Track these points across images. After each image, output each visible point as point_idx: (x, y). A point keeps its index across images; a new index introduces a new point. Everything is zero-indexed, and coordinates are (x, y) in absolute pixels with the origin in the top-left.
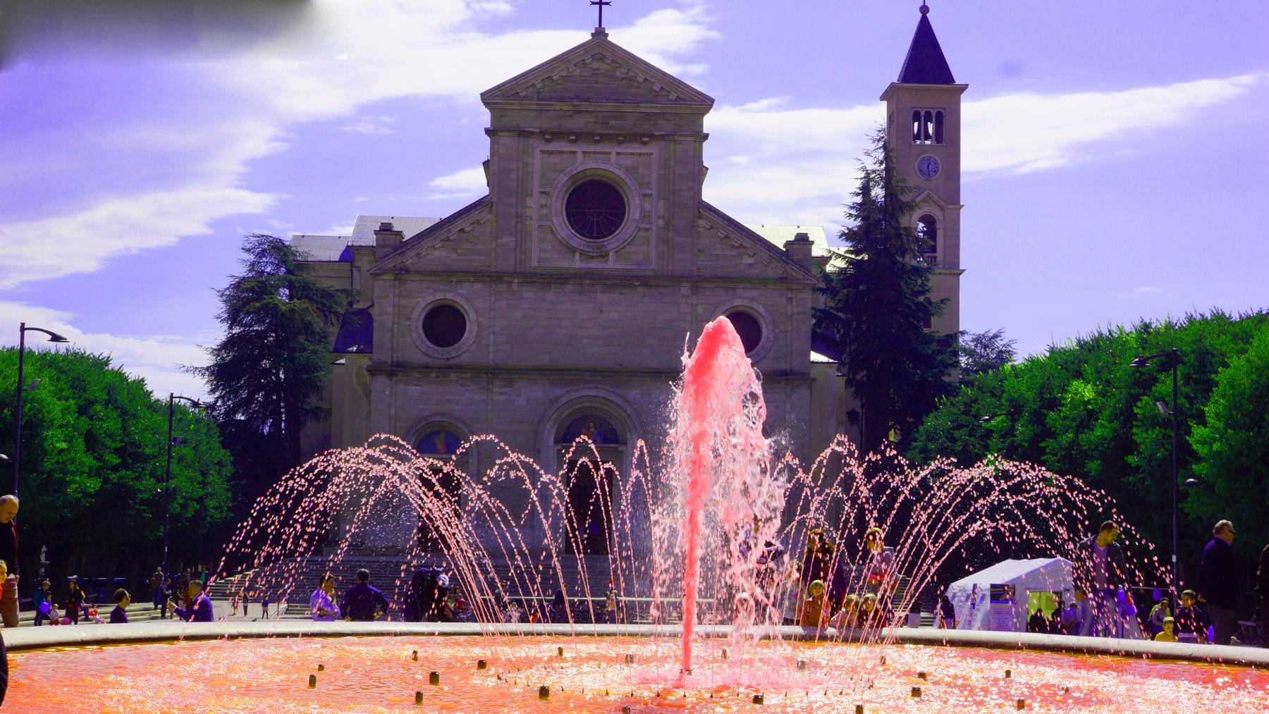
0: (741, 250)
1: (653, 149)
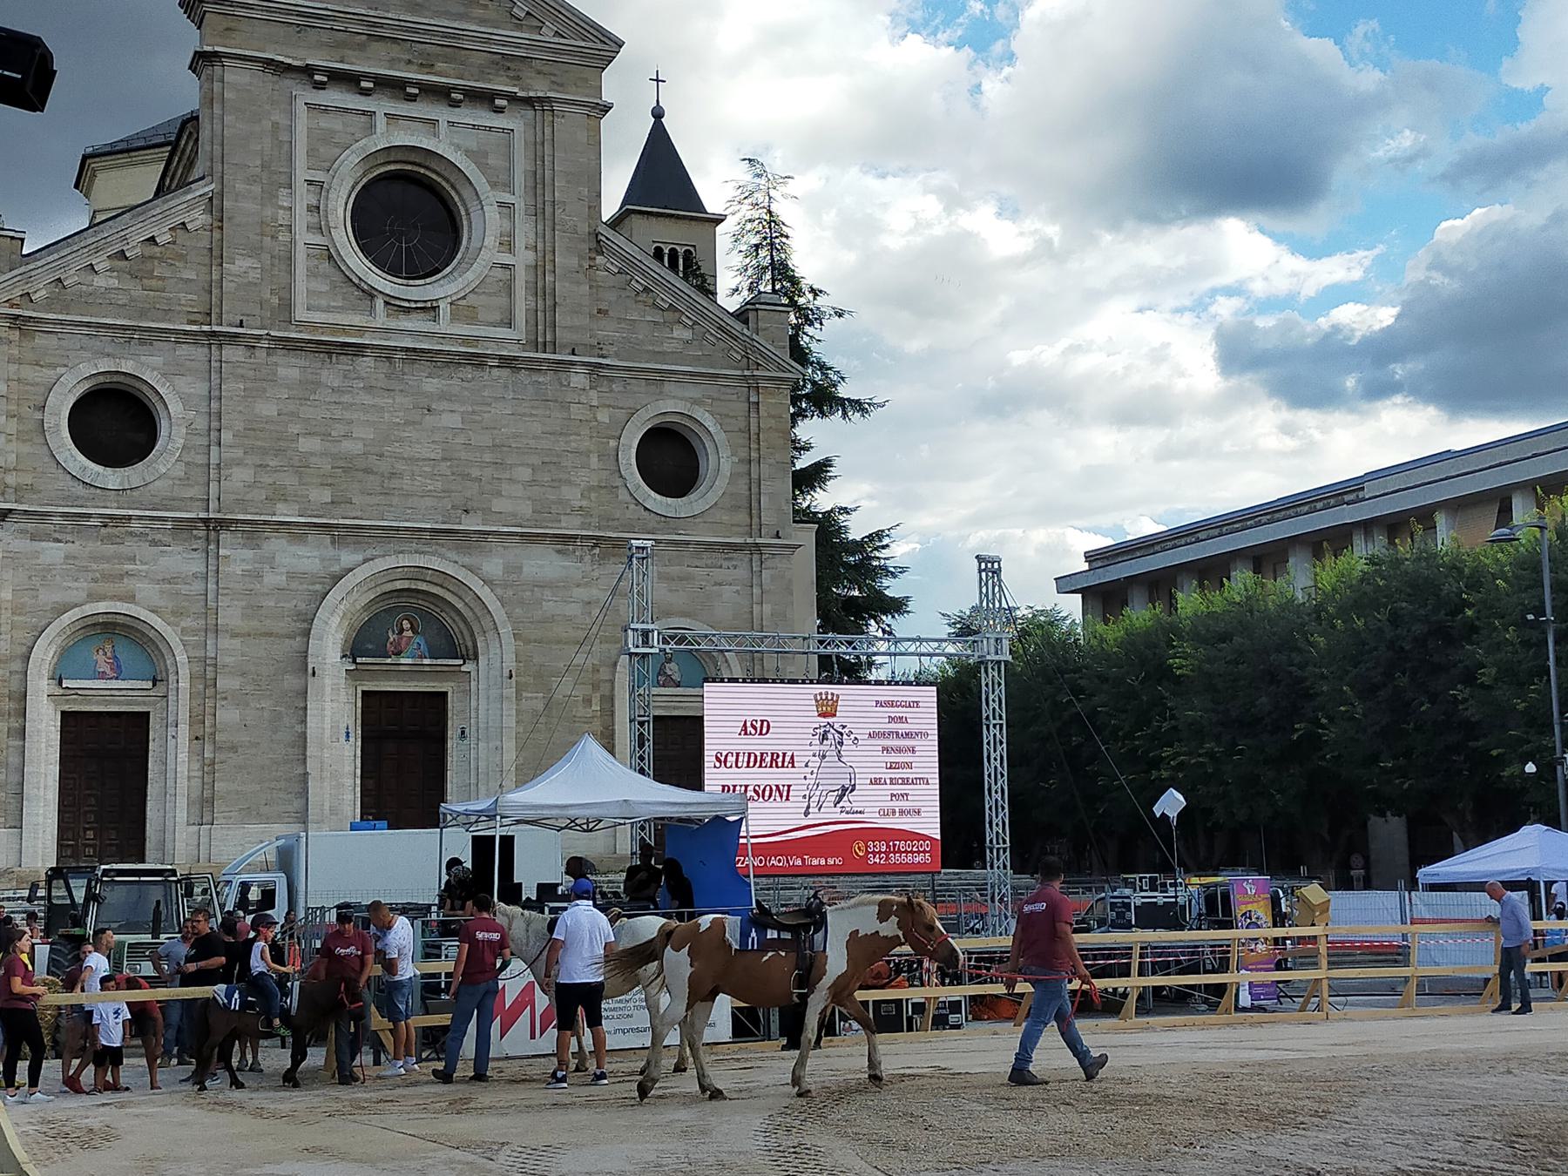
0: (670, 316)
1: (515, 122)
